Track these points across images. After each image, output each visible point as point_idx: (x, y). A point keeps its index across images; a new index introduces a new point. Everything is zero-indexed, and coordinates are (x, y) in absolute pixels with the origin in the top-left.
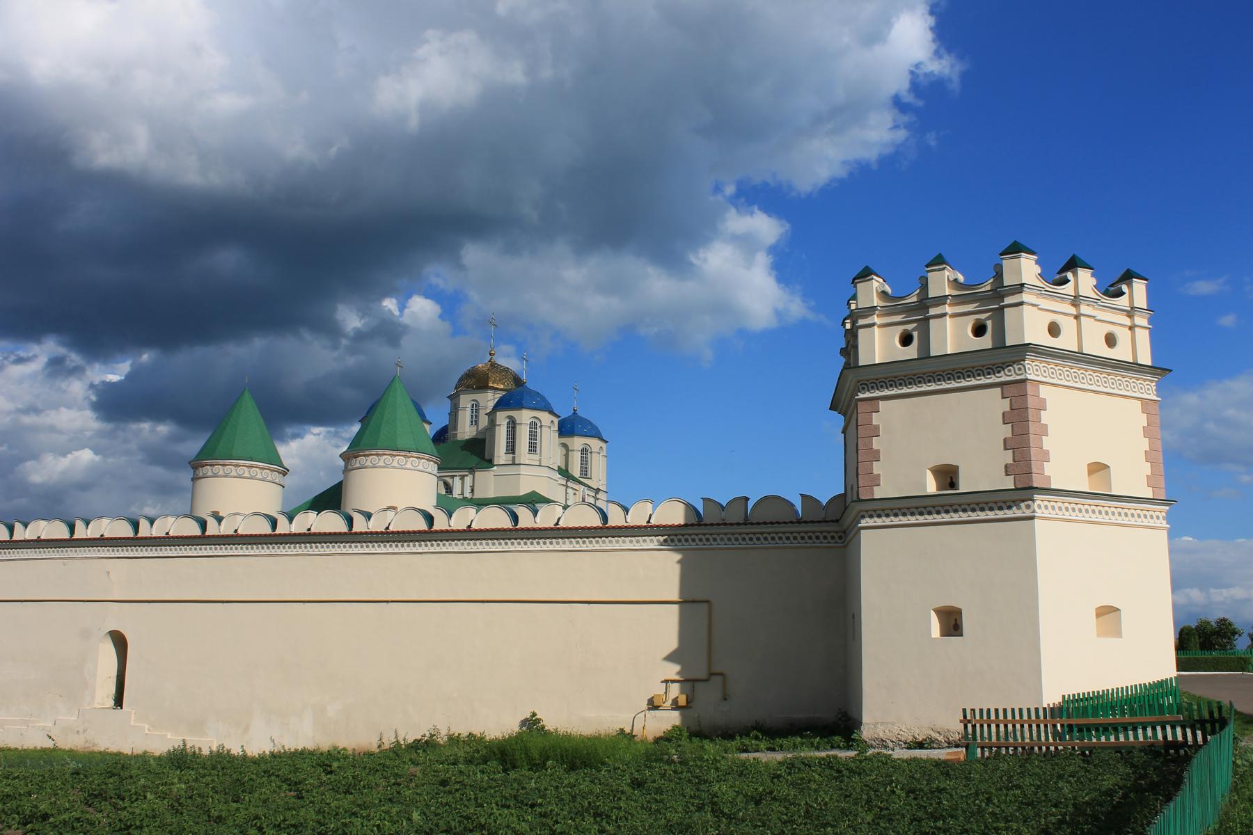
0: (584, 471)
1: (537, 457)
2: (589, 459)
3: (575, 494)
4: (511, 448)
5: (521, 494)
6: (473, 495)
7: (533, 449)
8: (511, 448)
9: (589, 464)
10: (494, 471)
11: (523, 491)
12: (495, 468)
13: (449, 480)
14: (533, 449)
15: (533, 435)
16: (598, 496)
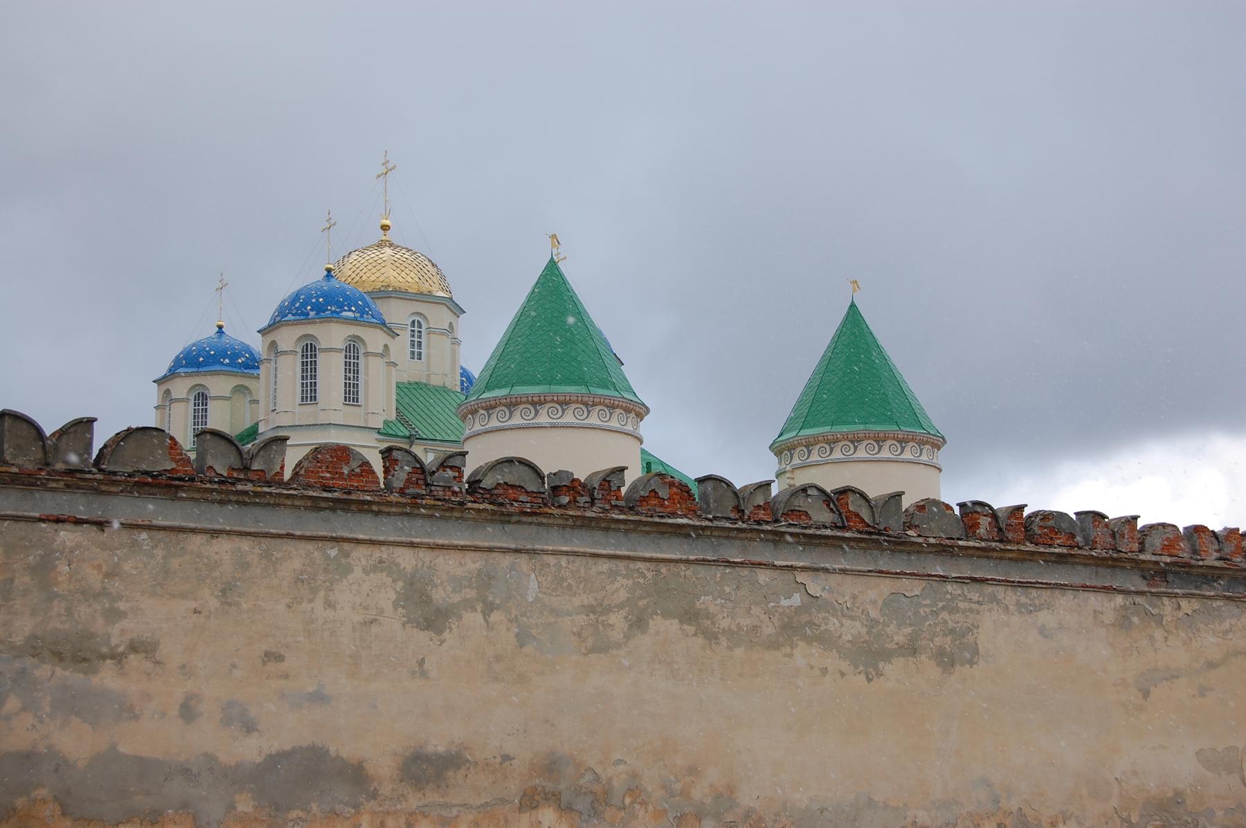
7: (310, 394)
14: (310, 394)
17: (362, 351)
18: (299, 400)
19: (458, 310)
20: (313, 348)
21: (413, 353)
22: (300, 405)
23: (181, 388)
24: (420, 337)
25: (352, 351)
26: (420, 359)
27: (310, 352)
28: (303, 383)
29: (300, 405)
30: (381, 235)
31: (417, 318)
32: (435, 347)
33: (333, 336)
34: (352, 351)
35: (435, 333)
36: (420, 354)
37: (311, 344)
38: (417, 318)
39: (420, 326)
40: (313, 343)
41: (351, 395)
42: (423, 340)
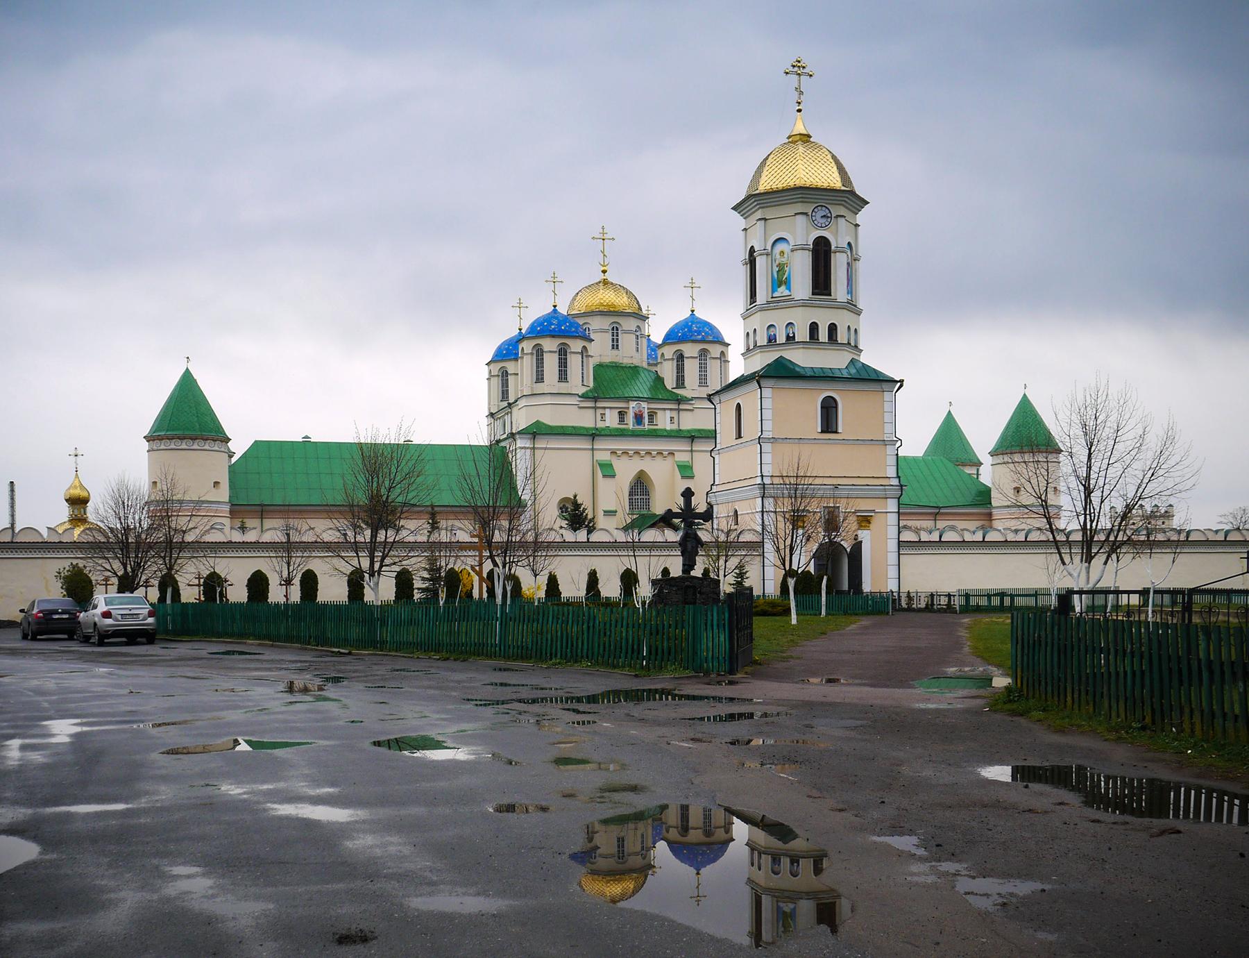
3: (622, 415)
7: (540, 378)
14: (540, 378)
17: (568, 351)
18: (535, 380)
19: (644, 318)
20: (542, 352)
21: (613, 345)
23: (496, 368)
24: (617, 336)
25: (563, 353)
26: (618, 348)
27: (539, 353)
30: (602, 276)
31: (615, 325)
32: (627, 341)
33: (549, 345)
34: (563, 353)
35: (625, 333)
36: (617, 345)
38: (615, 325)
39: (617, 329)
41: (563, 376)
42: (620, 337)
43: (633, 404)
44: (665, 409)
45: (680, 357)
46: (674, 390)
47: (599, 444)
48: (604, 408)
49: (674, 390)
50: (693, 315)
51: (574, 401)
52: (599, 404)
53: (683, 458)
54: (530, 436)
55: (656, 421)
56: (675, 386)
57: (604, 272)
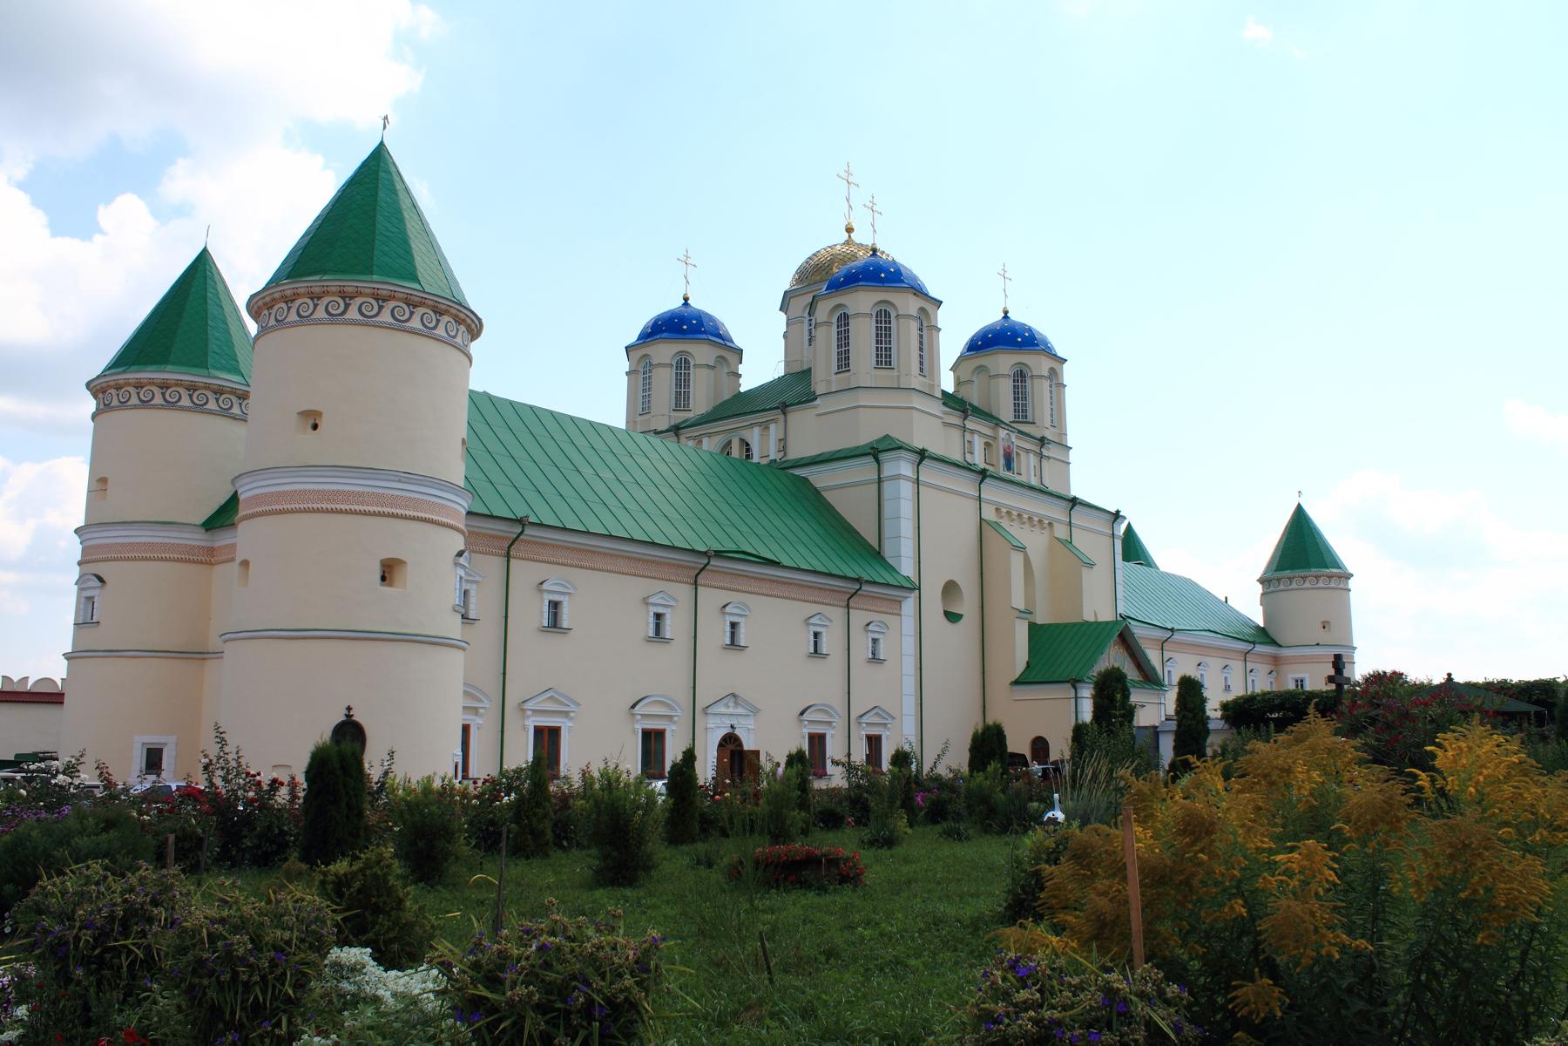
0: (1021, 411)
1: (895, 373)
2: (1029, 389)
4: (844, 362)
5: (862, 444)
6: (785, 455)
7: (884, 358)
8: (844, 362)
9: (1029, 399)
10: (815, 407)
11: (865, 437)
12: (818, 402)
13: (746, 434)
14: (884, 358)
15: (883, 335)
16: (1045, 452)
17: (925, 324)
20: (888, 315)
22: (875, 368)
28: (877, 348)
29: (875, 368)
37: (885, 310)
40: (888, 310)
43: (1002, 433)
44: (1028, 451)
45: (1020, 376)
46: (1013, 425)
47: (991, 491)
48: (972, 432)
49: (1014, 425)
50: (1006, 317)
51: (937, 408)
52: (969, 424)
53: (1061, 532)
54: (916, 458)
55: (1019, 468)
56: (1012, 419)
57: (849, 230)
